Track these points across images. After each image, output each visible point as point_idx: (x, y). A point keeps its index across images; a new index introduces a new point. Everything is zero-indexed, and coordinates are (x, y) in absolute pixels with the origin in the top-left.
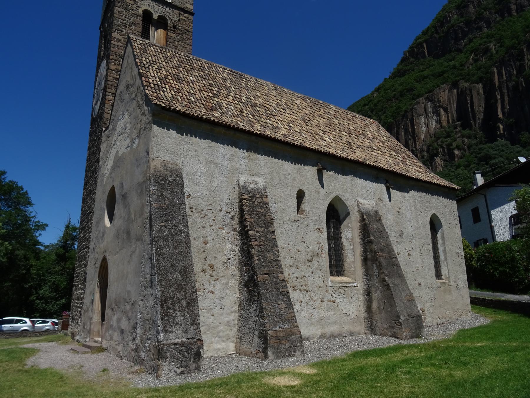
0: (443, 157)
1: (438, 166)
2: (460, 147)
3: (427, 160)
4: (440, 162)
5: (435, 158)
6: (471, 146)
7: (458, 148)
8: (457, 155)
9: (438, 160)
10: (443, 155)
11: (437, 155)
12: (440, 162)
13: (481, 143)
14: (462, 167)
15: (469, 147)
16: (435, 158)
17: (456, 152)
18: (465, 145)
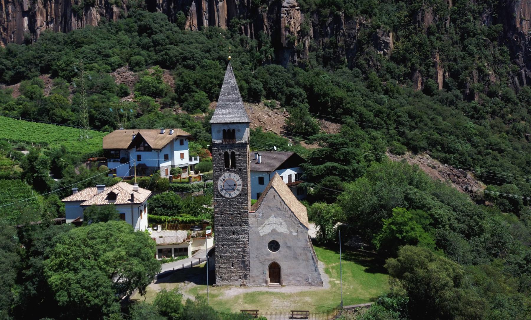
0: (99, 9)
1: (94, 19)
2: (119, 4)
3: (82, 8)
4: (95, 15)
5: (91, 8)
6: (130, 7)
7: (116, 3)
8: (115, 12)
9: (94, 11)
10: (99, 7)
11: (93, 5)
12: (95, 15)
13: (140, 6)
14: (123, 31)
15: (128, 7)
16: (91, 8)
17: (115, 9)
18: (124, 3)
